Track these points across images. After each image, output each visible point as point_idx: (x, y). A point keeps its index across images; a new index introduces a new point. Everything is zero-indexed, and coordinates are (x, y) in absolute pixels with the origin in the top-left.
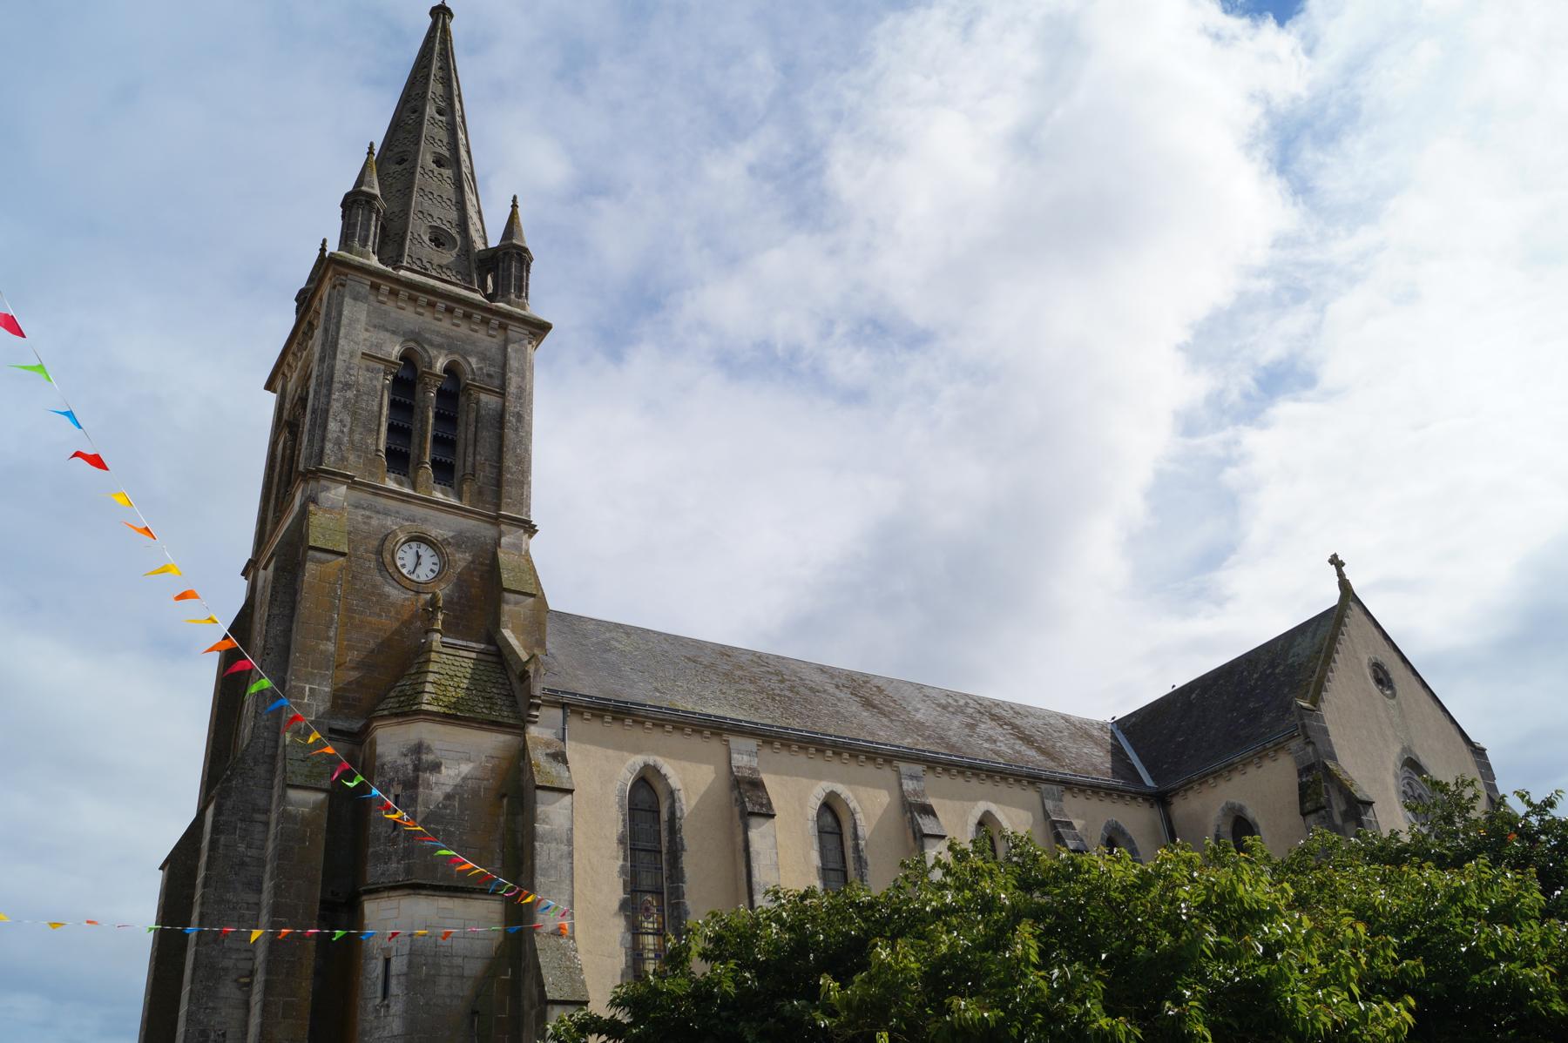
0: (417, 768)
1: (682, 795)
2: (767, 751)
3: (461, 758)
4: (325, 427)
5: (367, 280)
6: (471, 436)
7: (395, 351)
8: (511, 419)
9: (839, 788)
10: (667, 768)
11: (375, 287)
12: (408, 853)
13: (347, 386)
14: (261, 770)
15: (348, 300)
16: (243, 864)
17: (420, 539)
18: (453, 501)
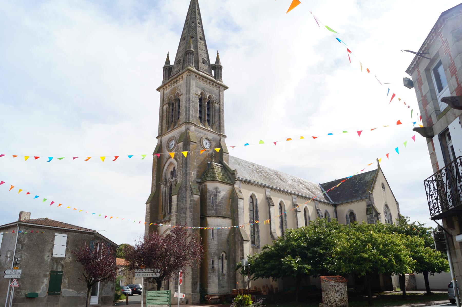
0: (217, 192)
1: (258, 200)
2: (271, 191)
3: (224, 190)
4: (189, 111)
5: (195, 75)
6: (214, 114)
7: (199, 93)
8: (221, 111)
9: (283, 200)
10: (256, 195)
11: (196, 76)
12: (216, 209)
13: (193, 102)
14: (184, 189)
15: (191, 80)
16: (182, 208)
17: (207, 139)
18: (212, 130)
